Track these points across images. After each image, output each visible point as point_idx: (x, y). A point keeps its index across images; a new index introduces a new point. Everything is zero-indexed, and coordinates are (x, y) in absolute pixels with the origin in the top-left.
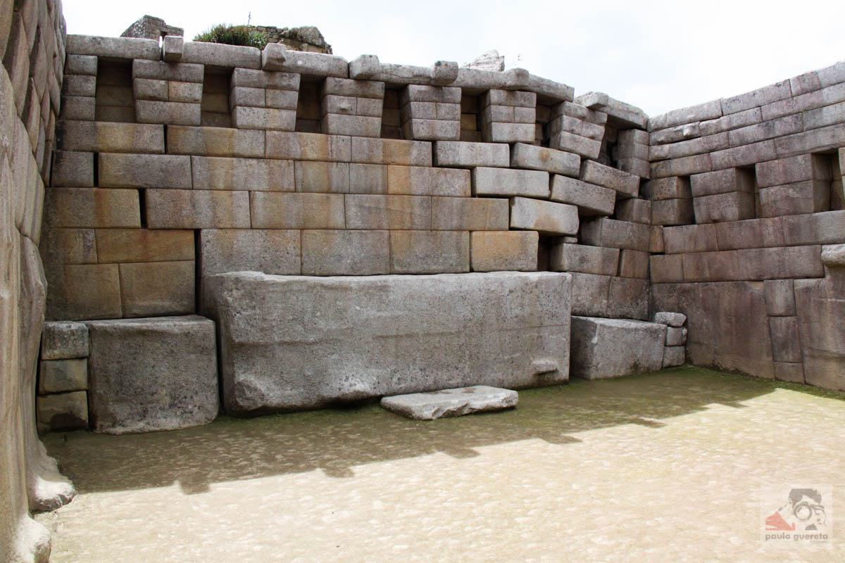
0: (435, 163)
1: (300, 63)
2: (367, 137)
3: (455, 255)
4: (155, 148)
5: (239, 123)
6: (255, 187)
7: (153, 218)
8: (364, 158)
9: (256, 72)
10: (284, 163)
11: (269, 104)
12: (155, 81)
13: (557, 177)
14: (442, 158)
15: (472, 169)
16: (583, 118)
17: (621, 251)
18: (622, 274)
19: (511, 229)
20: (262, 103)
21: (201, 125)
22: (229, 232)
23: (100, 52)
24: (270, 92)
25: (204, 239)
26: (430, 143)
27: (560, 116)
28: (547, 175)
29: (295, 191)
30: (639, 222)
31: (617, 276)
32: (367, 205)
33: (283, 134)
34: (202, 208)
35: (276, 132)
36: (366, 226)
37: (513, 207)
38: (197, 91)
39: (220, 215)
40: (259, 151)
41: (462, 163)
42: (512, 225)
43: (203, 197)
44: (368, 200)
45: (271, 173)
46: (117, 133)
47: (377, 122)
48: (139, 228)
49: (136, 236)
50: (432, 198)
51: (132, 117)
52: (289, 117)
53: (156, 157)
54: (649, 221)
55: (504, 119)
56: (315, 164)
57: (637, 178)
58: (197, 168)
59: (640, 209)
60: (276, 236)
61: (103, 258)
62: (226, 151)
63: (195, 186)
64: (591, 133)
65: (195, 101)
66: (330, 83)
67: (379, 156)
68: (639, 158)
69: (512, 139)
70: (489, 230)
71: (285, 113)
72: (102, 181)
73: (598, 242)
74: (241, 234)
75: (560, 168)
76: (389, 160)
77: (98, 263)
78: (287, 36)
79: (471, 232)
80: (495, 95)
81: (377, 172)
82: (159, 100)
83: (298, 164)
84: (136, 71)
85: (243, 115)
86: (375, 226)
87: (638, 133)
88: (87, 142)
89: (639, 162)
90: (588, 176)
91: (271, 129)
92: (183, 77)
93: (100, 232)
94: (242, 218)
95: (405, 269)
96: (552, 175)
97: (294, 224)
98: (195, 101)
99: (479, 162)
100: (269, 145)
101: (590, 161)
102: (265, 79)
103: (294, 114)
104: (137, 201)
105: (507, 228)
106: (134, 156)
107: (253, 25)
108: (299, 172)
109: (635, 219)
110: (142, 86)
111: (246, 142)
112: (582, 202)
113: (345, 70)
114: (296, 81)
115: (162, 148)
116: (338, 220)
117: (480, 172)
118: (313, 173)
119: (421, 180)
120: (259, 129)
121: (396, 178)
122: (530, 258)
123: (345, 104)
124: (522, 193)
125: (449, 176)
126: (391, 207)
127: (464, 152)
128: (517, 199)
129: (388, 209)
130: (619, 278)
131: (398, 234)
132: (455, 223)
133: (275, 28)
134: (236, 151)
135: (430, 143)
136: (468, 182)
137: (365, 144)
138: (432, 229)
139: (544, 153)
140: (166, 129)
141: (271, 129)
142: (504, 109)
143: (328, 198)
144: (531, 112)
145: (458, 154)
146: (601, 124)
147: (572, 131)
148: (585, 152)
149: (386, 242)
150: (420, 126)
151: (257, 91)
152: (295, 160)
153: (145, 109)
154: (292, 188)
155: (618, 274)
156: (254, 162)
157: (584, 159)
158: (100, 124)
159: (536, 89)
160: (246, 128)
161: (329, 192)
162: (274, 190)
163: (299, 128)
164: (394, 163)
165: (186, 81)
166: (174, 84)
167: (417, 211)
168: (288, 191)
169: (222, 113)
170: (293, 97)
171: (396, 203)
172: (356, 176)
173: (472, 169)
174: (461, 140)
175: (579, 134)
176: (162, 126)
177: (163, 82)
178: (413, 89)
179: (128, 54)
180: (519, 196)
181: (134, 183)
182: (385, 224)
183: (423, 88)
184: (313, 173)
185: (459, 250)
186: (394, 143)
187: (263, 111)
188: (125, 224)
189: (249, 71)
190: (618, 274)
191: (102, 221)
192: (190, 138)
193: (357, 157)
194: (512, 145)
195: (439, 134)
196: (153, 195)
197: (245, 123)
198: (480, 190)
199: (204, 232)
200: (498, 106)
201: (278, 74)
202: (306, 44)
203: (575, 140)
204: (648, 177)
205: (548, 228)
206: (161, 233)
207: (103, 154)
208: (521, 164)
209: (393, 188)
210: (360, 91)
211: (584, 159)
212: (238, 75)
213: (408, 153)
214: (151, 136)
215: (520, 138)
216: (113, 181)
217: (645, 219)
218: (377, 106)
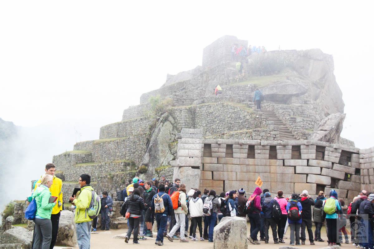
0: (284, 165)
1: (248, 143)
2: (265, 159)
3: (289, 189)
4: (215, 163)
5: (234, 157)
6: (238, 171)
7: (214, 178)
8: (264, 164)
9: (238, 145)
10: (244, 166)
11: (241, 152)
12: (216, 149)
13: (323, 168)
14: (286, 164)
16: (332, 152)
18: (348, 198)
19: (307, 183)
20: (239, 152)
21: (226, 157)
22: (231, 181)
23: (205, 143)
25: (225, 183)
26: (282, 160)
28: (320, 168)
29: (247, 172)
30: (355, 182)
31: (346, 198)
32: (265, 176)
33: (244, 159)
34: (225, 176)
35: (242, 159)
36: (265, 181)
37: (308, 177)
38: (224, 150)
39: (229, 177)
40: (239, 163)
41: (292, 165)
42: (307, 182)
43: (225, 173)
44: (265, 175)
45: (241, 168)
47: (268, 156)
48: (211, 180)
49: (211, 181)
50: (283, 174)
51: (211, 156)
52: (246, 155)
53: (215, 164)
54: (360, 182)
55: (305, 153)
56: (252, 166)
57: (354, 169)
58: (225, 167)
59: (355, 178)
60: (242, 182)
61: (204, 186)
62: (231, 163)
63: (224, 171)
64: (335, 156)
65: (224, 152)
66: (256, 147)
67: (268, 164)
68: (355, 162)
69: (308, 158)
71: (245, 154)
72: (204, 169)
73: (339, 188)
74: (234, 182)
76: (271, 165)
77: (203, 187)
78: (302, 55)
79: (294, 183)
80: (302, 147)
81: (268, 168)
82: (216, 152)
83: (248, 166)
84: (212, 147)
85: (235, 155)
86: (267, 181)
87: (354, 155)
89: (355, 164)
90: (334, 168)
91: (241, 158)
92: (222, 147)
93: (203, 180)
94: (234, 178)
95: (275, 192)
96: (321, 168)
97: (246, 180)
98: (224, 152)
99: (297, 164)
100: (241, 162)
101: (335, 164)
102: (240, 147)
103: (247, 154)
104: (211, 174)
105: (306, 182)
106: (211, 164)
107: (282, 50)
108: (248, 168)
109: (353, 181)
110: (213, 149)
111: (235, 161)
112: (332, 176)
113: (259, 144)
114: (247, 147)
115: (217, 163)
117: (297, 168)
118: (251, 168)
119: (280, 169)
120: (238, 158)
121: (273, 169)
122: (313, 191)
123: (259, 152)
124: (311, 173)
125: (288, 169)
126: (271, 176)
127: (293, 162)
128: (309, 175)
129: (270, 177)
130: (346, 199)
131: (273, 183)
132: (289, 181)
133: (295, 50)
134: (233, 163)
135: (282, 160)
136: (294, 170)
137: (264, 161)
138: (283, 182)
139: (318, 162)
140: (218, 158)
141: (241, 158)
142: (305, 151)
143: (255, 174)
145: (290, 163)
146: (339, 153)
147: (329, 155)
148: (333, 161)
149: (270, 185)
150: (279, 156)
151: (238, 149)
152: (247, 165)
153: (213, 154)
154: (246, 171)
155: (347, 197)
156: (237, 165)
157: (333, 163)
158: (204, 158)
159: (316, 144)
160: (235, 158)
161: (255, 172)
162: (242, 172)
163: (248, 158)
165: (223, 148)
166: (219, 149)
167: (279, 177)
168: (245, 172)
169: (231, 154)
170: (246, 151)
171: (273, 175)
172: (261, 169)
173: (295, 167)
174: (292, 159)
175: (331, 156)
176: (217, 158)
177: (217, 149)
178: (278, 147)
179: (210, 143)
181: (211, 170)
182: (269, 180)
183: (281, 146)
184: (251, 168)
185: (290, 188)
186: (273, 161)
187: (239, 154)
188: (209, 179)
189: (236, 145)
190: (347, 197)
191: (204, 178)
192: (223, 160)
193: (262, 164)
194: (308, 160)
195: (285, 158)
196: (215, 173)
197: (235, 157)
198: (297, 172)
199: (225, 181)
200: (303, 150)
201: (243, 145)
202: (313, 60)
203: (329, 158)
205: (319, 183)
206: (216, 181)
207: (204, 164)
208: (310, 165)
209: (272, 172)
210: (263, 148)
211: (333, 163)
212: (234, 146)
213: (276, 163)
214: (215, 160)
215: (310, 158)
216: (206, 170)
217: (358, 181)
218: (268, 152)
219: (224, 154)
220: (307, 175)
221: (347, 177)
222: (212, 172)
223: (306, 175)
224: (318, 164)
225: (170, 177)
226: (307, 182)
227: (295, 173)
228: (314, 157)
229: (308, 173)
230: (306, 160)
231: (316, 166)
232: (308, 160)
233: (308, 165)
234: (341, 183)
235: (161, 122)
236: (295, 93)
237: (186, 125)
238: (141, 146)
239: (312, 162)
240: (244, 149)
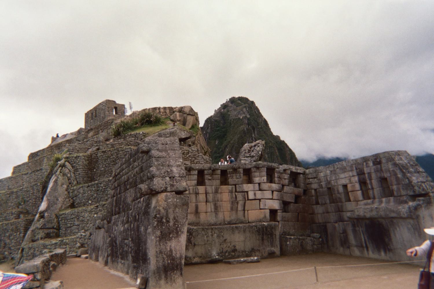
13: (274, 192)
15: (247, 192)
17: (298, 214)
24: (190, 176)
27: (274, 173)
28: (271, 192)
56: (203, 195)
70: (253, 210)
75: (274, 189)
79: (248, 211)
96: (273, 192)
103: (196, 181)
105: (259, 209)
116: (209, 210)
124: (263, 198)
128: (262, 200)
144: (264, 173)
150: (230, 181)
157: (283, 186)
159: (266, 166)
164: (224, 192)
173: (247, 192)
180: (262, 199)
194: (259, 184)
195: (236, 183)
204: (306, 189)
205: (272, 208)
208: (262, 189)
209: (224, 200)
221: (297, 198)
223: (258, 201)
224: (270, 187)
225: (72, 220)
228: (265, 181)
229: (261, 198)
230: (258, 184)
231: (267, 189)
233: (260, 190)
234: (292, 207)
235: (60, 166)
236: (183, 137)
237: (84, 170)
238: (35, 194)
239: (265, 186)
240: (193, 175)
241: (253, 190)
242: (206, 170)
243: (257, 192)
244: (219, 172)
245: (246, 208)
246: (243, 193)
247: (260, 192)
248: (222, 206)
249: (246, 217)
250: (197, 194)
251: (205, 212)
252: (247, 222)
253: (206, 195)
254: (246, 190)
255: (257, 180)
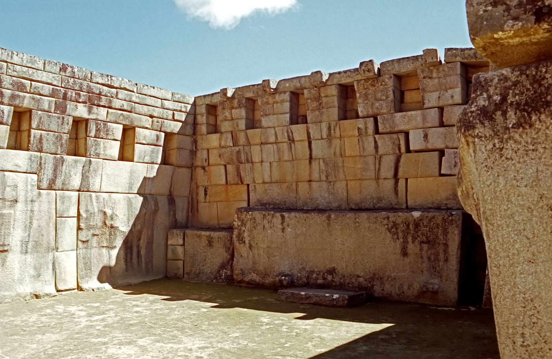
19: (441, 175)
42: (442, 172)
46: (214, 140)
88: (205, 146)
104: (223, 171)
105: (437, 173)
166: (233, 111)
194: (441, 109)
219: (242, 124)
220: (442, 153)
222: (225, 166)
226: (442, 172)
227: (408, 151)
232: (441, 109)
233: (442, 125)
241: (421, 125)
242: (305, 88)
243: (431, 132)
244: (333, 91)
245: (400, 174)
246: (395, 136)
247: (442, 130)
248: (343, 166)
249: (400, 193)
250: (291, 140)
251: (308, 180)
252: (404, 206)
253: (310, 143)
254: (402, 127)
255: (432, 99)
